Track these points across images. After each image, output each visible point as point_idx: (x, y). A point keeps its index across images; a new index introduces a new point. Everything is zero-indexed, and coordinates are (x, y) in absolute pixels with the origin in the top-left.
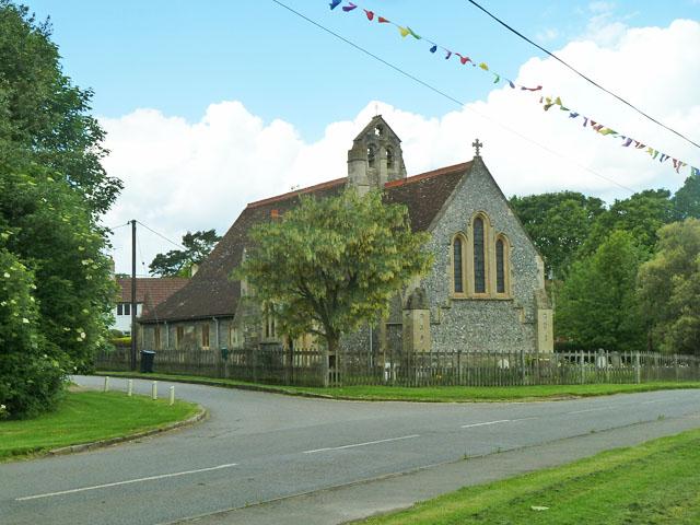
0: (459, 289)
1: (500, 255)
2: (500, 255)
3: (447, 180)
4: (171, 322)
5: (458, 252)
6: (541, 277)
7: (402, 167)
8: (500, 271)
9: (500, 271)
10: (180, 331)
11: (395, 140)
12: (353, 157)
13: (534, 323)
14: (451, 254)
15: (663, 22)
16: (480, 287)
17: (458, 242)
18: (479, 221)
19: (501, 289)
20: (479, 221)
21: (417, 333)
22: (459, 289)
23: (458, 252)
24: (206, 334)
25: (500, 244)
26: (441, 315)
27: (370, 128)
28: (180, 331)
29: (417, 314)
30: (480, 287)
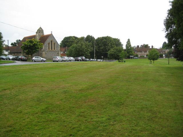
0: (49, 49)
1: (54, 46)
2: (54, 46)
3: (48, 36)
4: (13, 53)
5: (49, 45)
6: (59, 48)
7: (44, 34)
8: (54, 47)
9: (54, 47)
10: (15, 54)
11: (43, 30)
12: (37, 33)
13: (58, 54)
14: (48, 45)
15: (98, 38)
16: (52, 49)
17: (49, 44)
18: (52, 41)
19: (54, 49)
20: (52, 41)
21: (44, 55)
22: (49, 49)
23: (49, 45)
24: (18, 55)
25: (54, 44)
26: (46, 52)
27: (39, 29)
28: (15, 54)
29: (44, 52)
30: (52, 49)
